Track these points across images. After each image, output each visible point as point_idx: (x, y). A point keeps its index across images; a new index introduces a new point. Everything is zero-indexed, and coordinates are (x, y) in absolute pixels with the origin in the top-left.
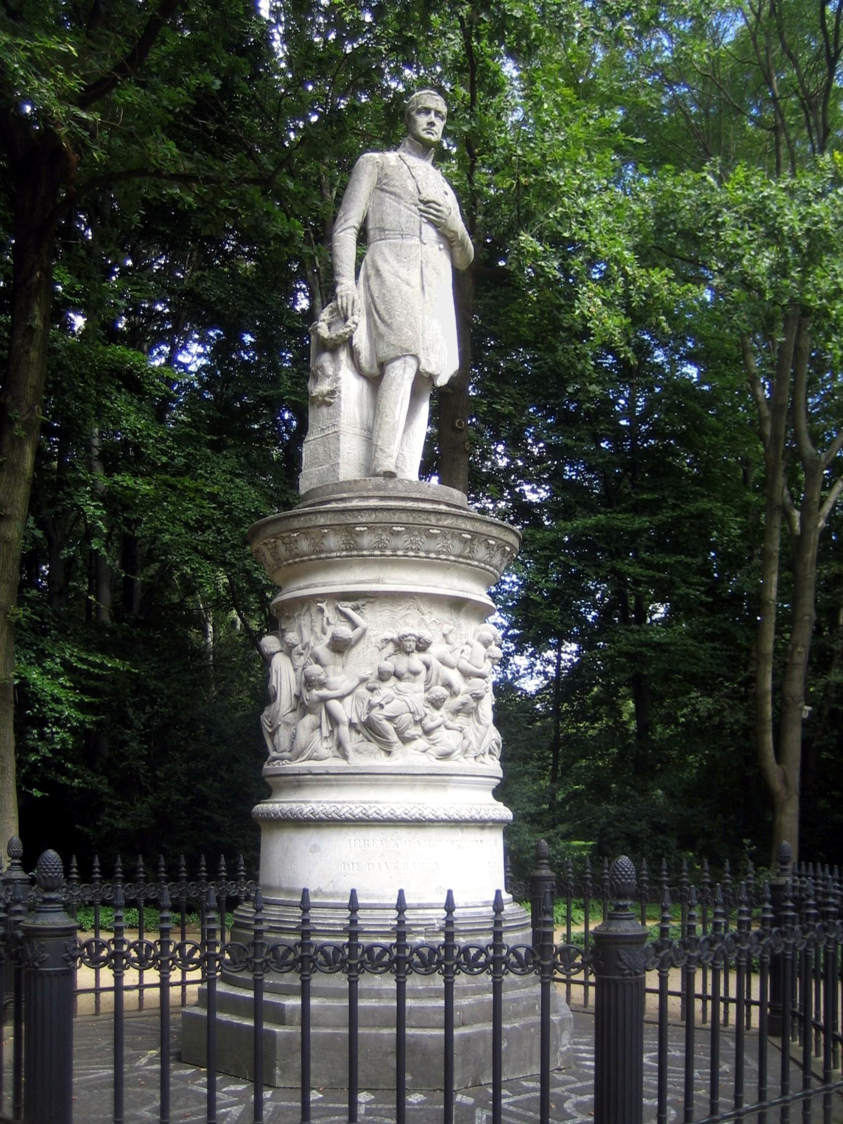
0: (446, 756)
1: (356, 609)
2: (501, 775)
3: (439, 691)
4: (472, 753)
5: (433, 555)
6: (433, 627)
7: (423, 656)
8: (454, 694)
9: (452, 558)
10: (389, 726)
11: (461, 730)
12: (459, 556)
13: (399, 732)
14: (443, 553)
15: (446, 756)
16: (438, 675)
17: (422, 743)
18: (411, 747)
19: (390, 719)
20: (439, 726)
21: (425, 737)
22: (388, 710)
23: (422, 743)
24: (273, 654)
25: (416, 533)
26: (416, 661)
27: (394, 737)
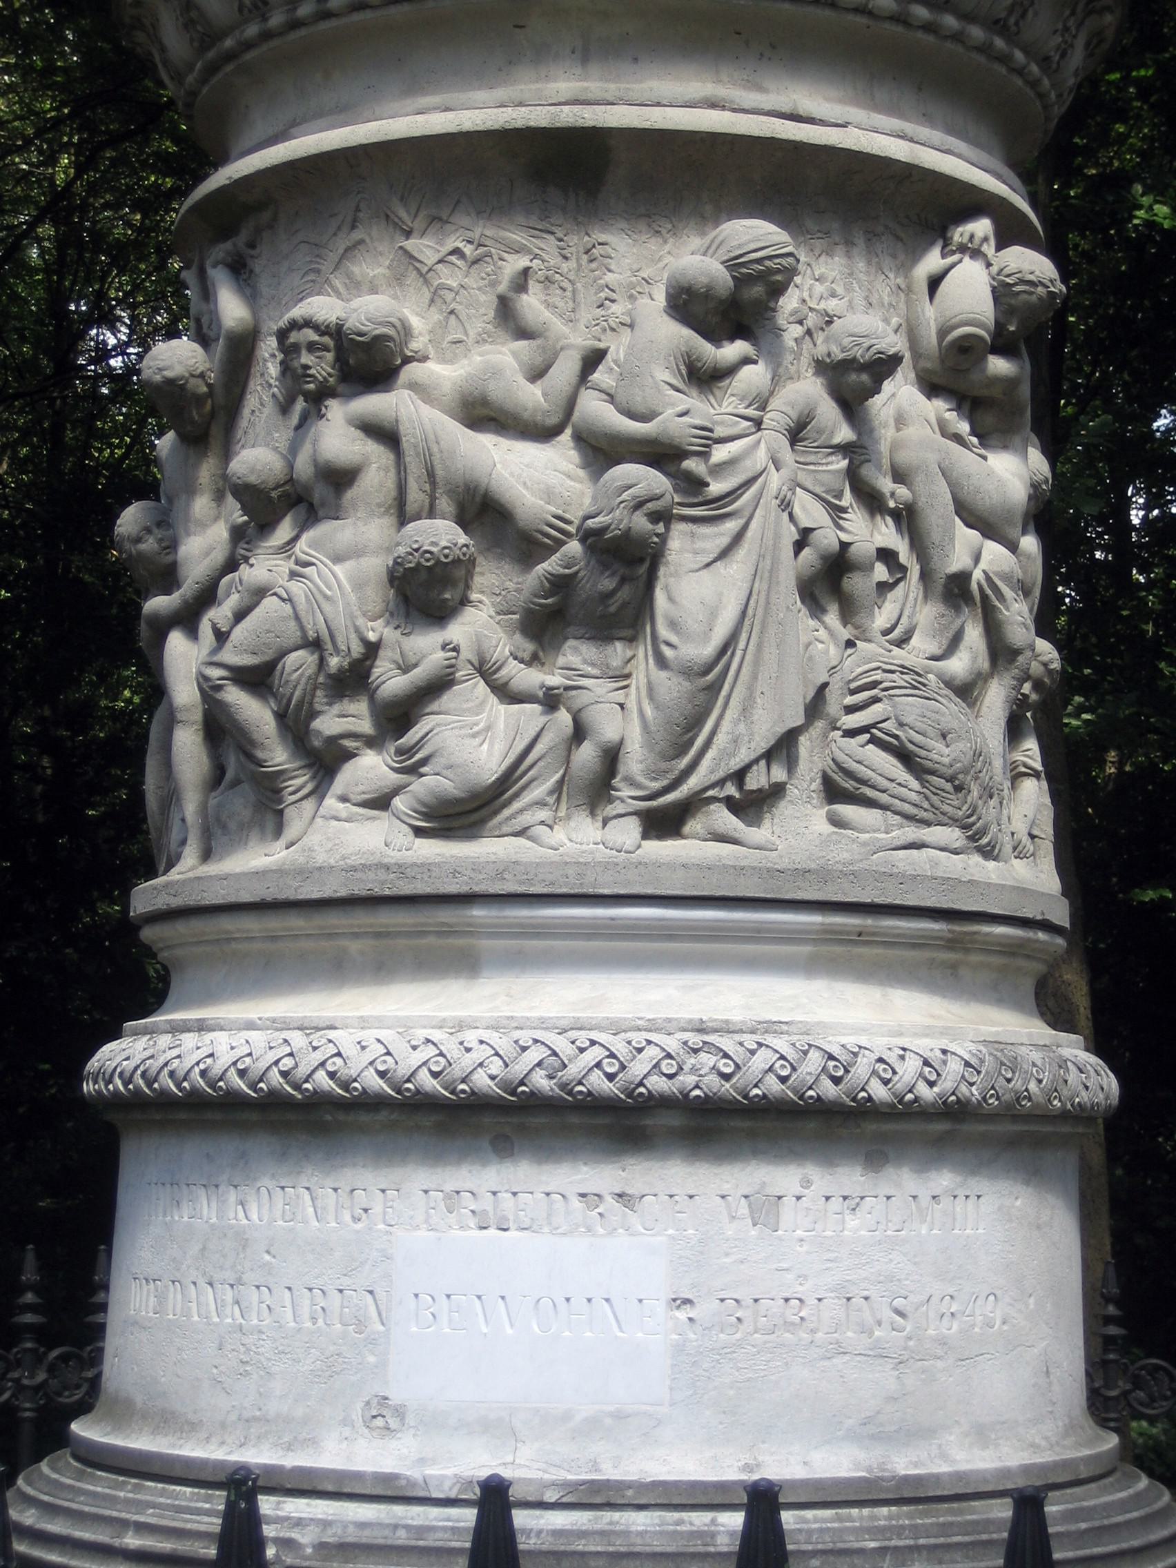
0: (460, 815)
6: (449, 277)
7: (373, 404)
10: (254, 712)
13: (295, 724)
15: (460, 815)
16: (431, 475)
17: (371, 768)
19: (258, 679)
20: (438, 685)
23: (371, 768)
27: (278, 756)
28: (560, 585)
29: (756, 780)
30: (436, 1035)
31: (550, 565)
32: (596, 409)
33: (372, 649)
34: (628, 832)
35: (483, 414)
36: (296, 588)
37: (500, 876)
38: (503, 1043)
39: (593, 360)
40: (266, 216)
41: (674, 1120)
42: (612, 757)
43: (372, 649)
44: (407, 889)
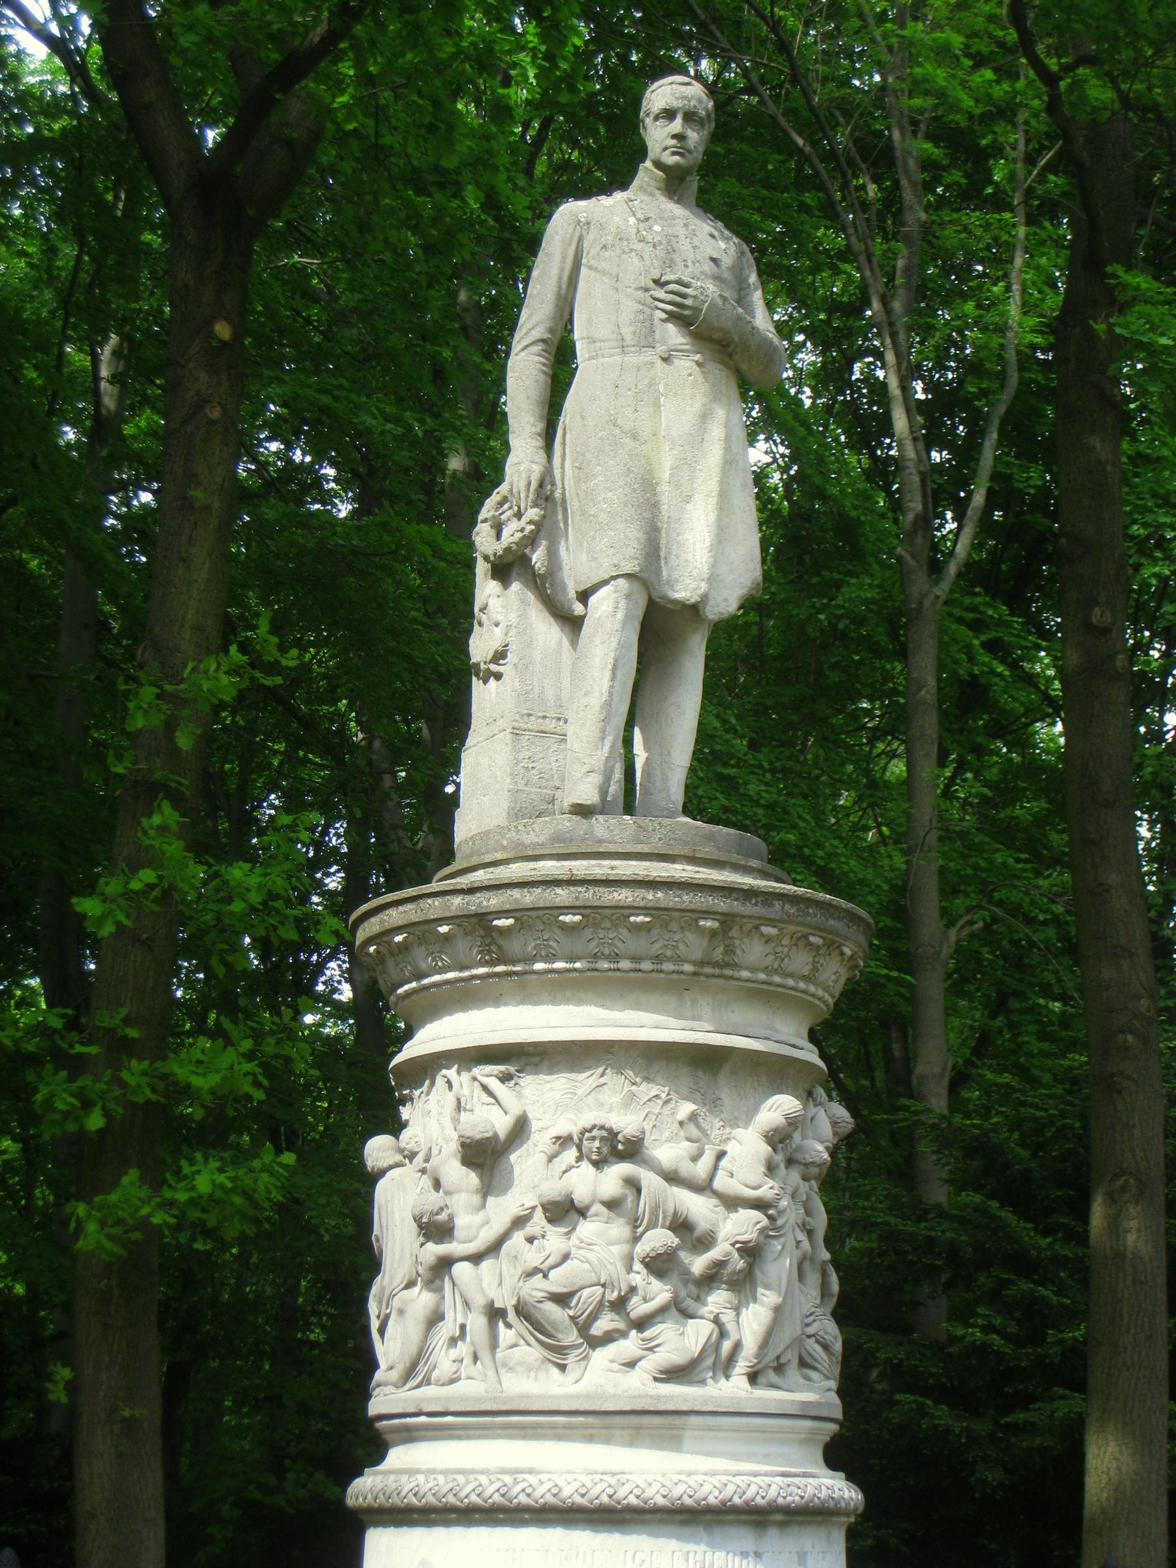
1: (505, 1078)
2: (839, 1415)
4: (742, 1366)
5: (646, 965)
8: (704, 1242)
9: (688, 968)
12: (702, 963)
14: (669, 959)
18: (601, 1357)
19: (562, 1299)
21: (633, 1333)
22: (558, 1280)
24: (382, 1173)
25: (607, 924)
26: (611, 1179)
28: (720, 1264)
30: (683, 1477)
31: (715, 1254)
32: (721, 1182)
33: (633, 1290)
35: (672, 1178)
36: (591, 1256)
37: (705, 1402)
38: (613, 1481)
39: (721, 1155)
40: (537, 1059)
41: (779, 1517)
42: (737, 1346)
43: (633, 1290)
44: (662, 1408)
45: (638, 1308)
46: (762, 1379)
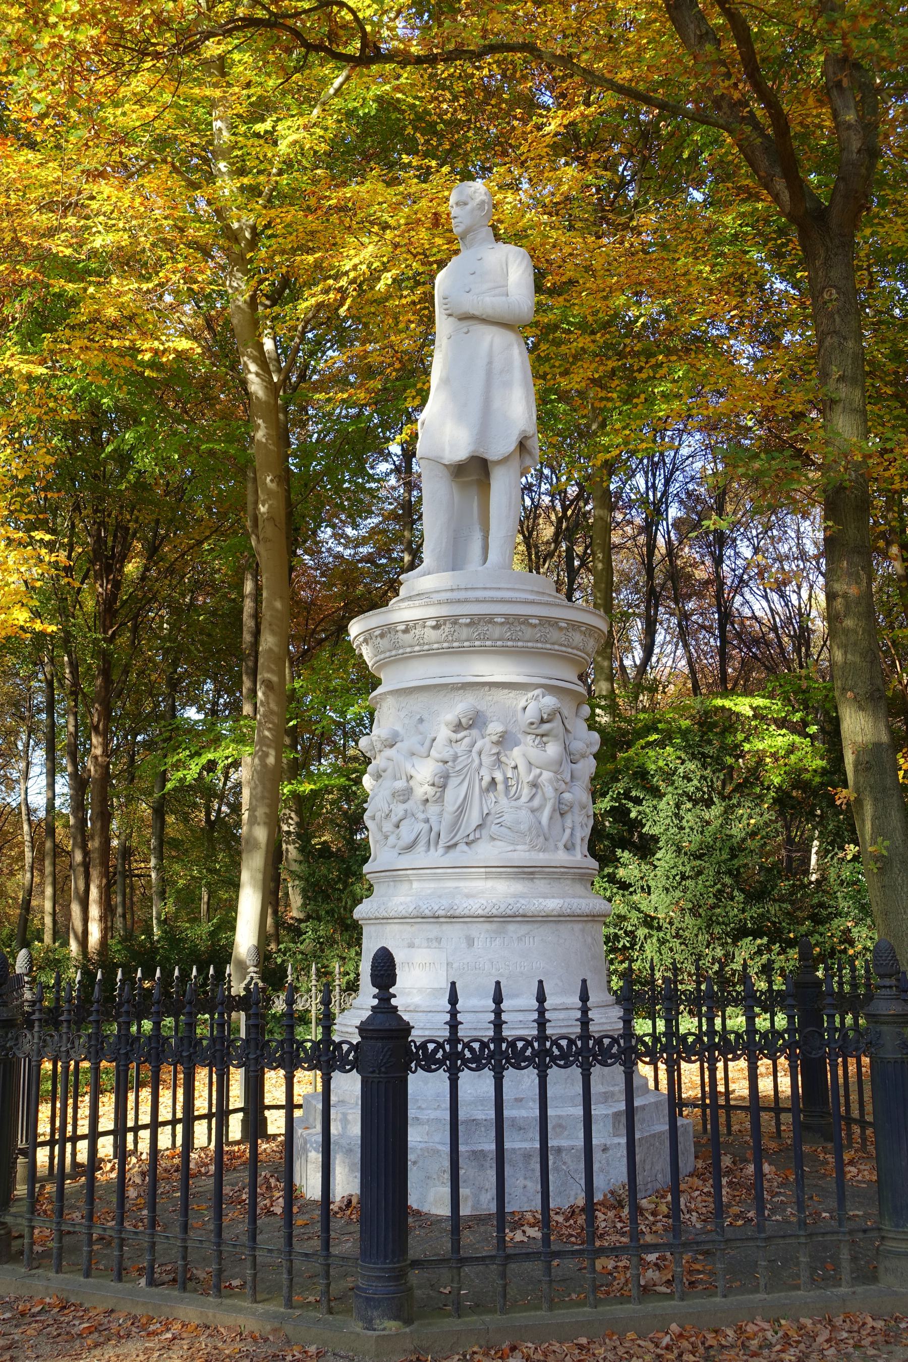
3: (400, 784)
11: (427, 821)
29: (471, 837)
34: (441, 851)
45: (394, 819)
46: (459, 848)
